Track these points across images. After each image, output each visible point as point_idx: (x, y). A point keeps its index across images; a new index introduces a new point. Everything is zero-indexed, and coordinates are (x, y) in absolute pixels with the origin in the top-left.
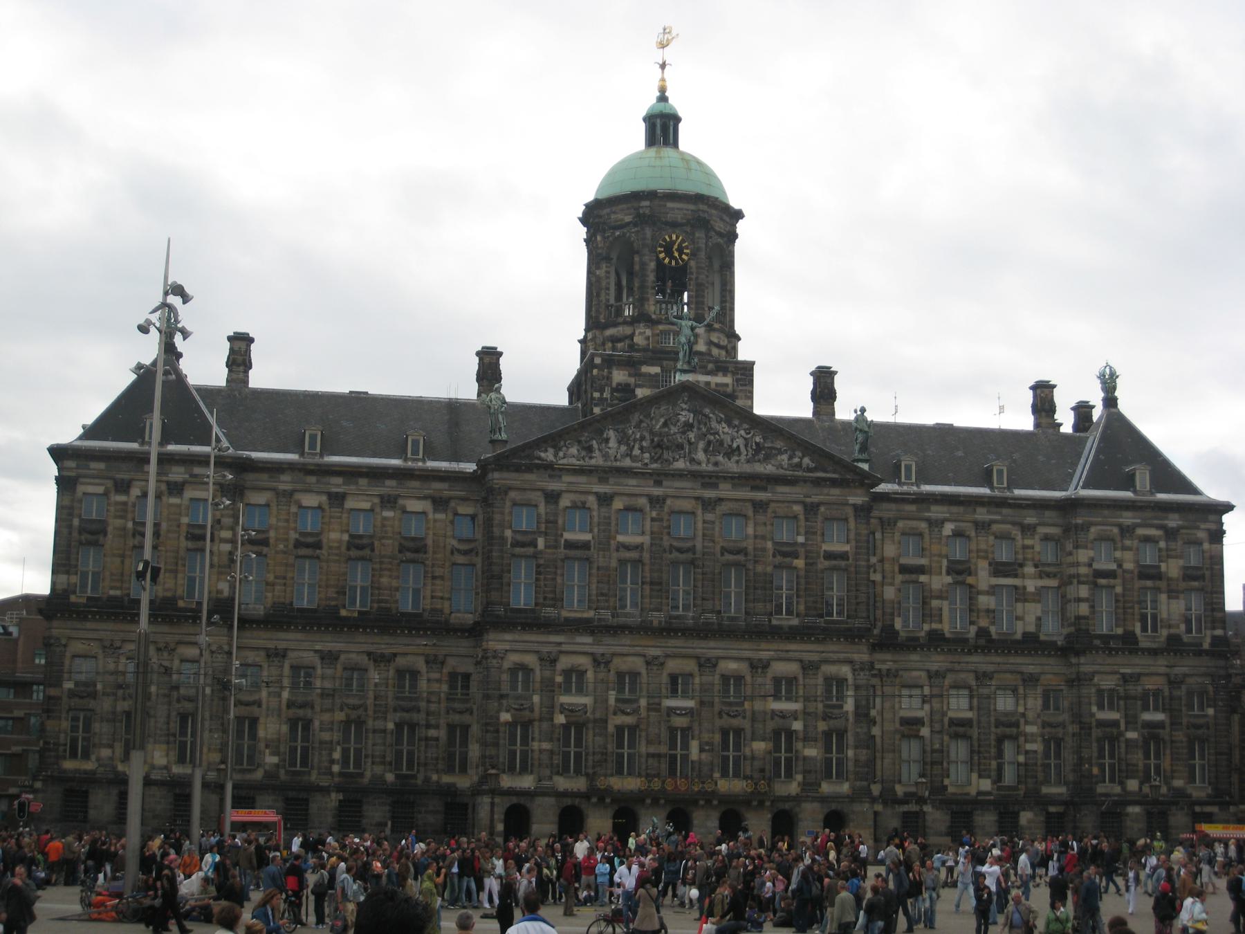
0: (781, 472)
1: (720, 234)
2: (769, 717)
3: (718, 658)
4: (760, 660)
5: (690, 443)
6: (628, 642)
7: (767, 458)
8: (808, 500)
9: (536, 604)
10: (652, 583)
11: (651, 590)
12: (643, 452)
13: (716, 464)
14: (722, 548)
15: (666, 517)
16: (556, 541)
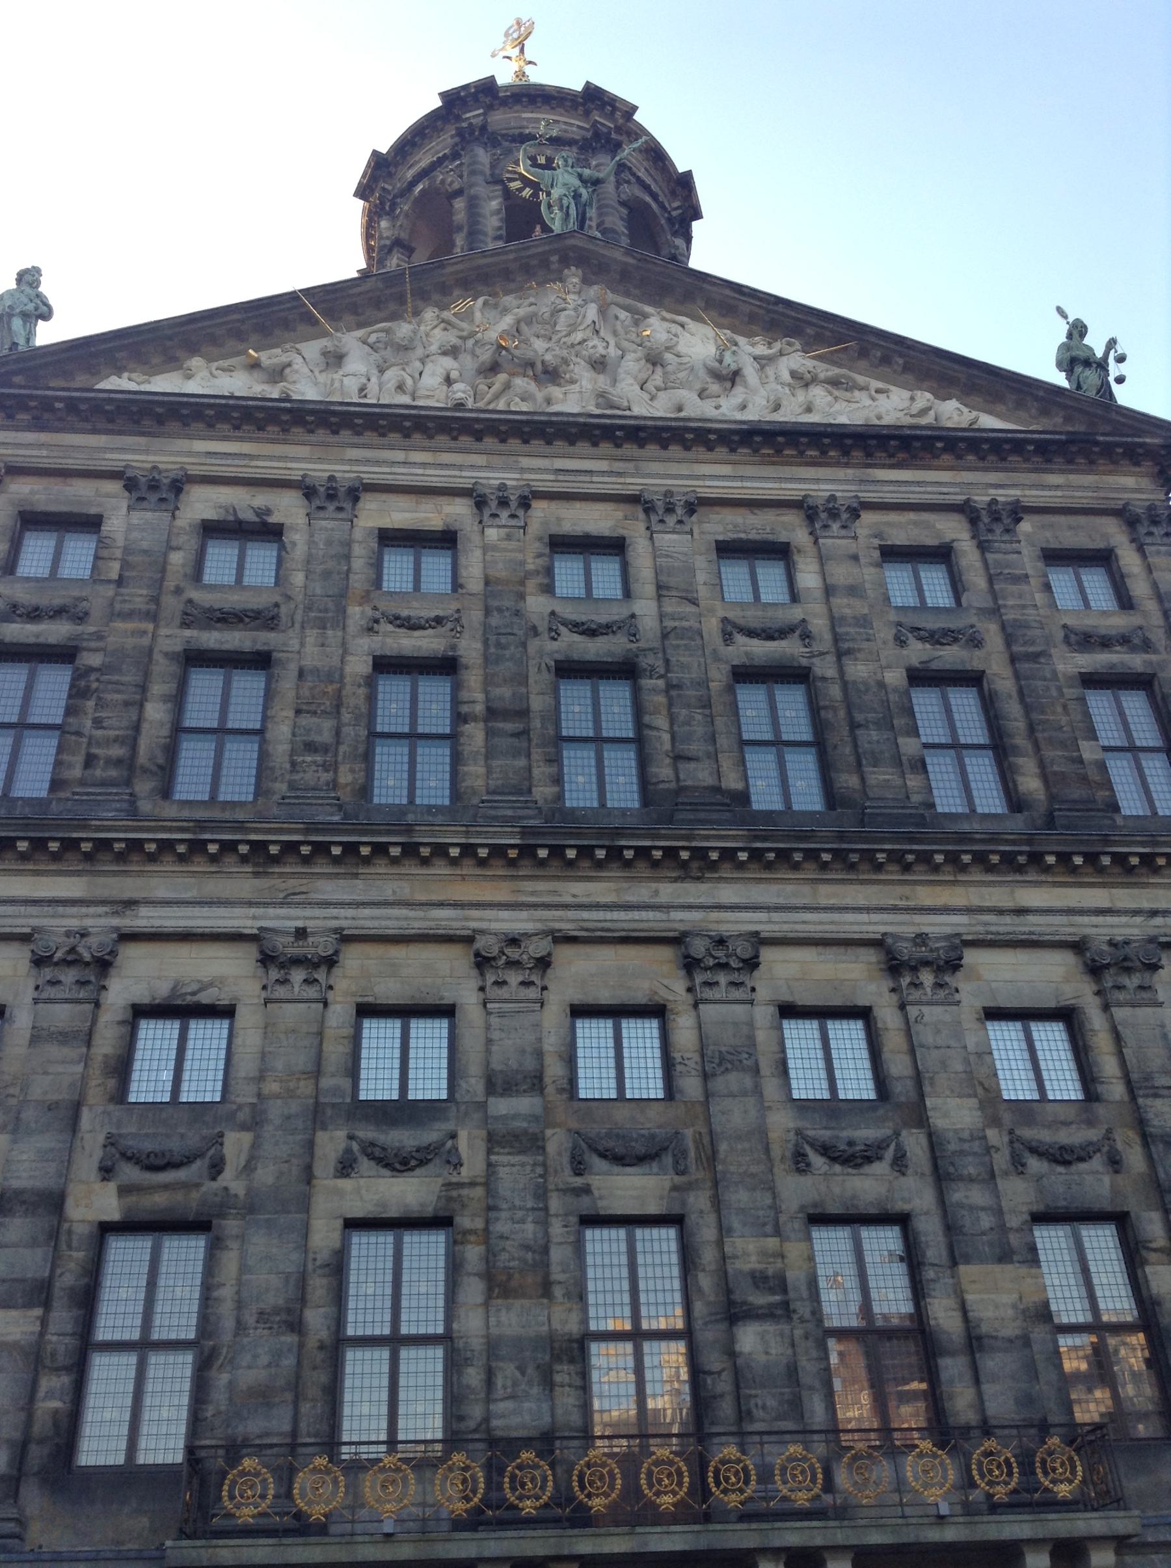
1: (647, 188)
2: (1001, 1160)
3: (759, 941)
4: (921, 939)
8: (981, 499)
9: (56, 784)
10: (492, 713)
11: (490, 733)
14: (725, 620)
16: (156, 600)
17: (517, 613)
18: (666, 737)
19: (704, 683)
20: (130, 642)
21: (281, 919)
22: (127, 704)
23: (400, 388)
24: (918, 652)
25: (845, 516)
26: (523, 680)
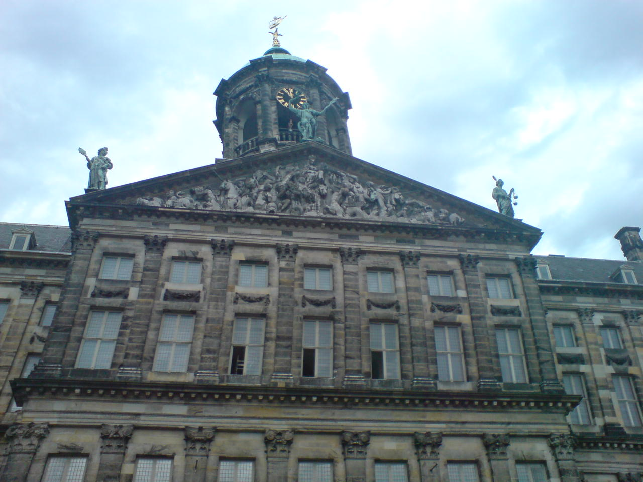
0: (427, 223)
5: (323, 196)
6: (240, 414)
7: (410, 214)
10: (278, 338)
11: (277, 346)
12: (268, 202)
13: (354, 214)
14: (368, 300)
15: (298, 269)
16: (154, 290)
17: (291, 297)
18: (343, 348)
19: (358, 327)
20: (144, 307)
21: (195, 423)
22: (141, 333)
23: (249, 205)
24: (438, 314)
25: (415, 259)
26: (290, 324)
